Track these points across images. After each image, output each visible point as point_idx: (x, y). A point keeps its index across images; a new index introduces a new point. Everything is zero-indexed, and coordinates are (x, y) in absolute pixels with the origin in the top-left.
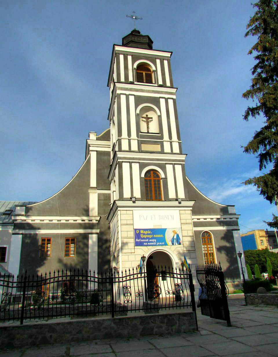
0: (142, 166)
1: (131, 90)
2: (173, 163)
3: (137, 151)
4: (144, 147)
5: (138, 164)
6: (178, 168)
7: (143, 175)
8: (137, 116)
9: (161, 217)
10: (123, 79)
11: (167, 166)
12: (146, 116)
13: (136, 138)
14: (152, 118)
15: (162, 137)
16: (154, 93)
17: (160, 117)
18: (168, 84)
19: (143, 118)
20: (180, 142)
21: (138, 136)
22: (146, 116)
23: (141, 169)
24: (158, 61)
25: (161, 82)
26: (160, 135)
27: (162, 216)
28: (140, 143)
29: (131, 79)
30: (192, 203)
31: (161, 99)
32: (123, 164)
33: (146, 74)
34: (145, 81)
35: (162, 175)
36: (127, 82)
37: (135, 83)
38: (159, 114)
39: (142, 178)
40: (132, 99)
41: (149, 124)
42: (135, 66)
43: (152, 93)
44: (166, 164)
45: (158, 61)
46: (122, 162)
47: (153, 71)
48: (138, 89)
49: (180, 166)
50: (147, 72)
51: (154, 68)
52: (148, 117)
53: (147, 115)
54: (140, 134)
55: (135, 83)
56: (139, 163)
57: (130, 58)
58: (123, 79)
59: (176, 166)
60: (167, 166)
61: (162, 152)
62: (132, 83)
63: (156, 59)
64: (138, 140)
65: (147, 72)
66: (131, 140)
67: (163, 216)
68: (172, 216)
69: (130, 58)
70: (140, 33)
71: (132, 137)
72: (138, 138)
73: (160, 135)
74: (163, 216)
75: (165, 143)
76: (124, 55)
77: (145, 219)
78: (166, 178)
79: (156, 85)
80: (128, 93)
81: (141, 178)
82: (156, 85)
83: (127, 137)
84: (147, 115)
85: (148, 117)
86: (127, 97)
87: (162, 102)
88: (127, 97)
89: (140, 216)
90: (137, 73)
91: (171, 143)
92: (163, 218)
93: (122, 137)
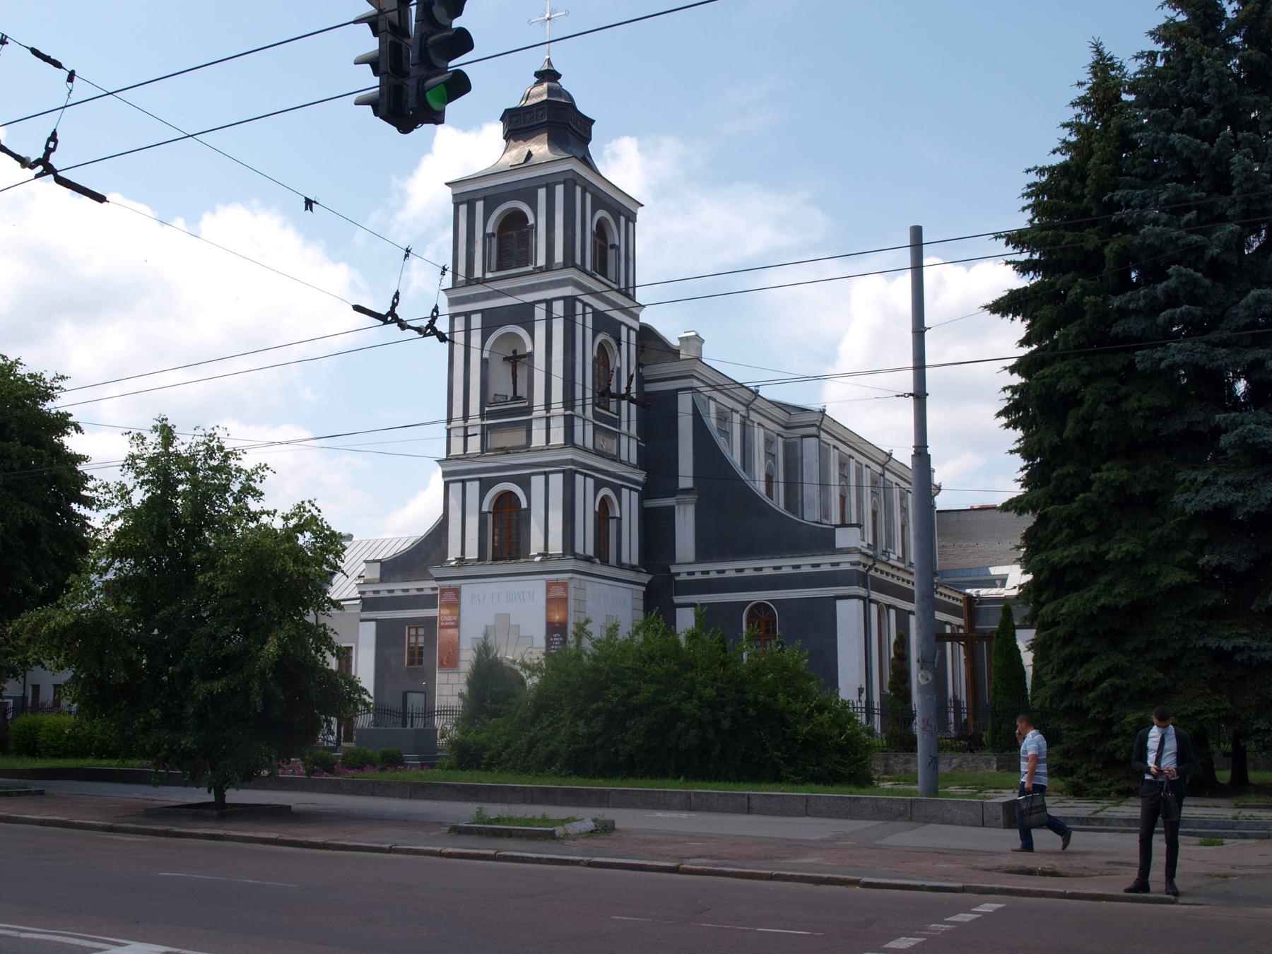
0: (599, 485)
2: (631, 485)
6: (635, 495)
10: (578, 261)
15: (617, 423)
21: (595, 413)
24: (623, 219)
30: (646, 578)
38: (618, 365)
44: (623, 486)
45: (623, 219)
46: (576, 472)
47: (613, 246)
51: (617, 243)
54: (597, 409)
58: (578, 261)
61: (615, 459)
73: (618, 417)
78: (620, 519)
79: (615, 286)
81: (595, 512)
82: (615, 286)
83: (581, 413)
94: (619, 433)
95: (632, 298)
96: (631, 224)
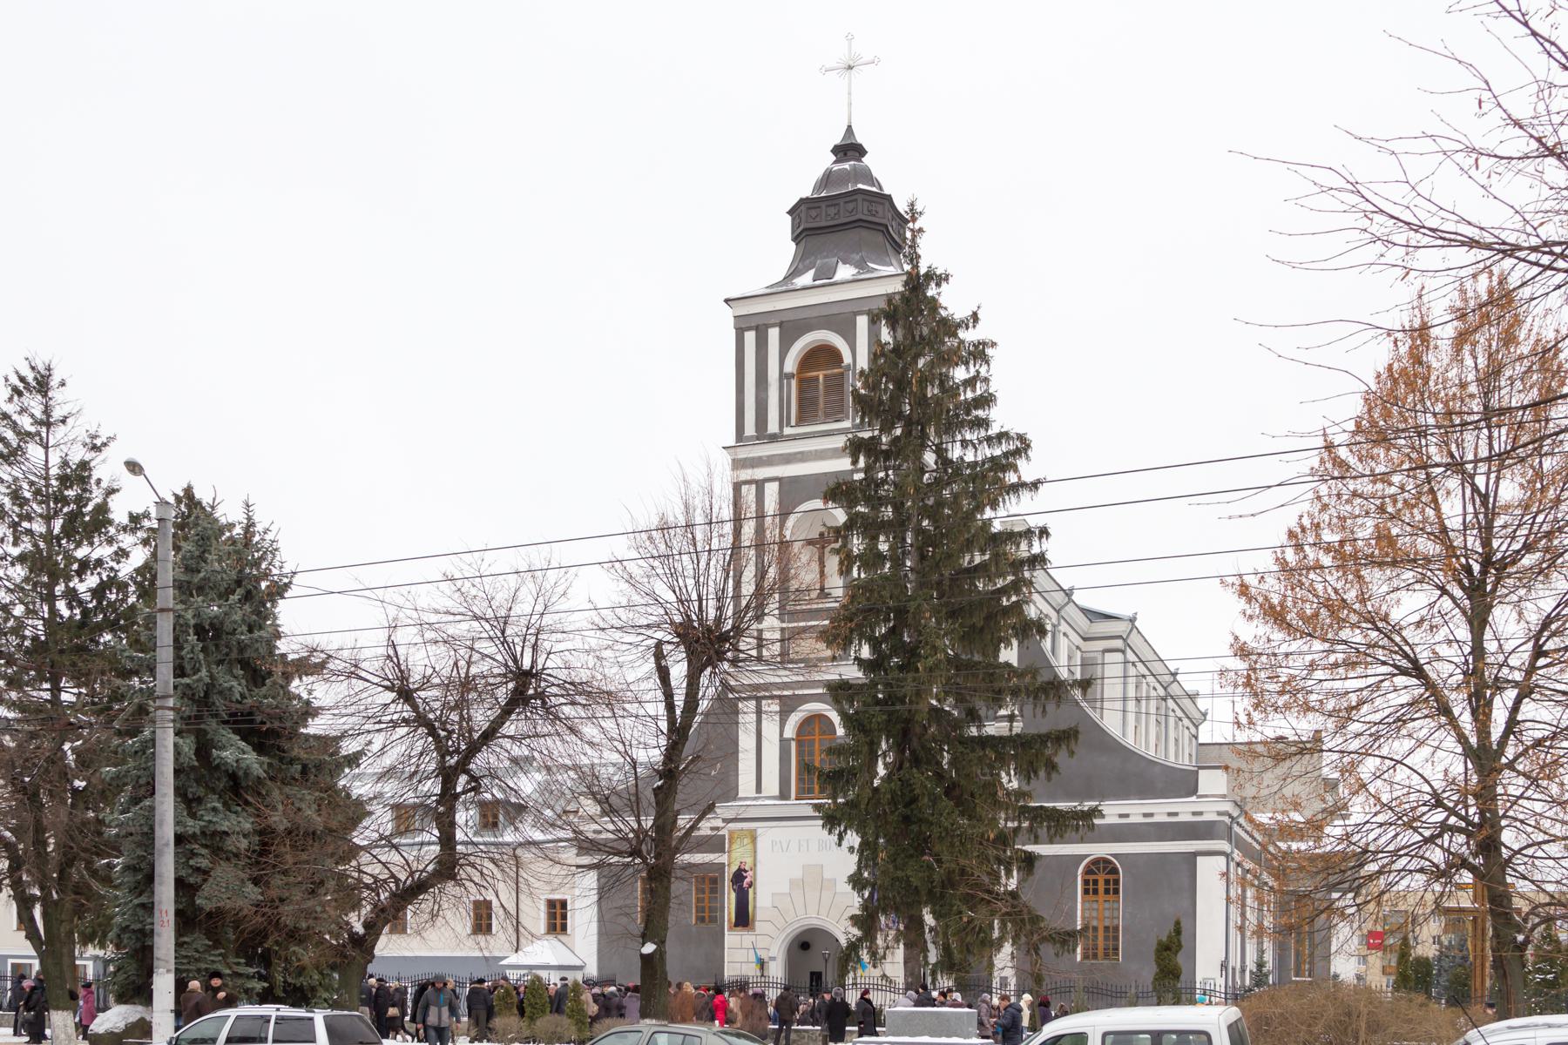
7: (790, 732)
23: (784, 715)
33: (825, 376)
37: (787, 431)
39: (789, 740)
42: (791, 365)
43: (831, 458)
48: (790, 454)
50: (829, 372)
55: (787, 431)
56: (780, 697)
57: (774, 334)
65: (829, 372)
69: (774, 334)
76: (757, 328)
77: (785, 847)
86: (760, 485)
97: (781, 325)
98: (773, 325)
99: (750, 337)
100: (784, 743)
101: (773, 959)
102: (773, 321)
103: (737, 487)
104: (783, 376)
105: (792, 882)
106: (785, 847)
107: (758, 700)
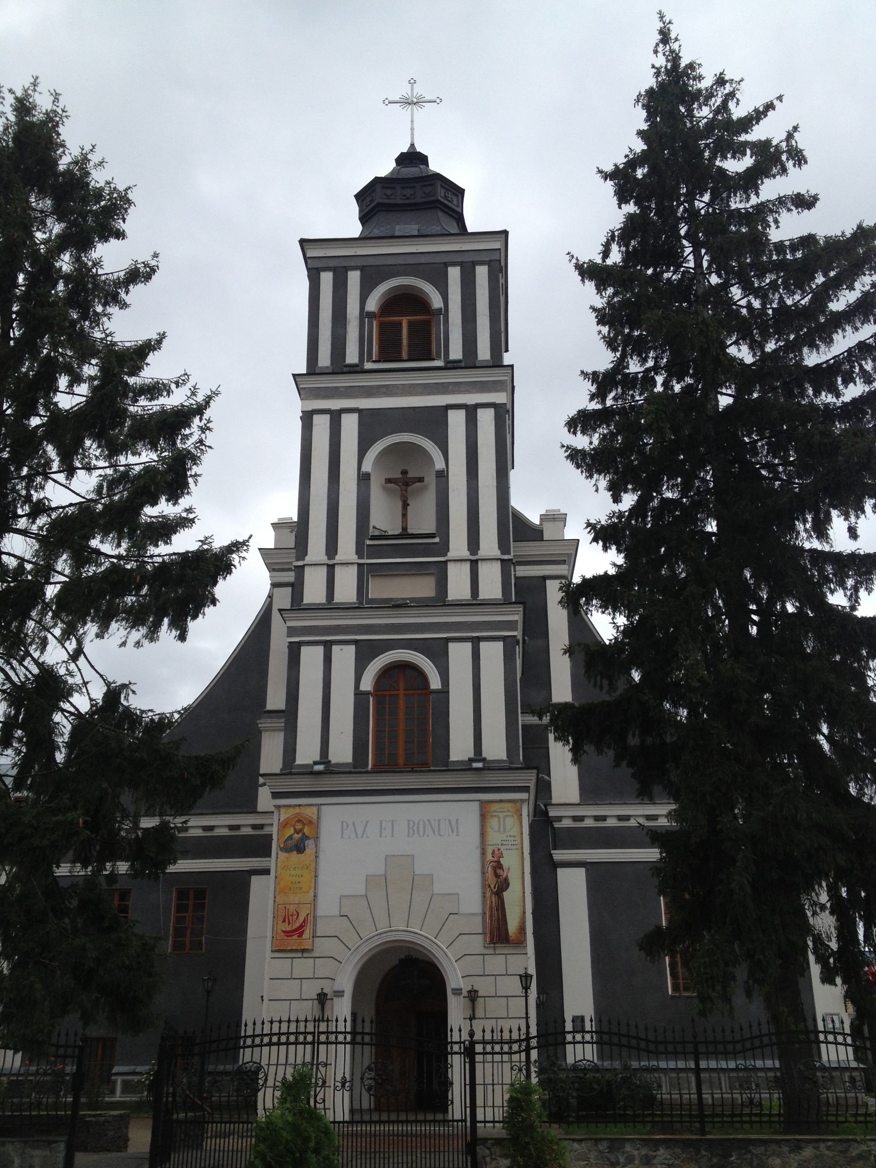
1: (348, 392)
3: (354, 603)
4: (378, 589)
5: (352, 648)
7: (367, 685)
8: (364, 479)
9: (415, 828)
11: (451, 646)
12: (400, 476)
13: (354, 558)
14: (421, 480)
15: (444, 547)
16: (429, 394)
17: (442, 476)
18: (484, 352)
19: (391, 483)
20: (506, 557)
21: (359, 552)
22: (400, 476)
24: (454, 274)
25: (456, 352)
26: (437, 540)
27: (416, 824)
28: (364, 573)
29: (352, 356)
31: (451, 413)
32: (304, 650)
33: (411, 324)
34: (405, 355)
35: (435, 683)
36: (340, 367)
38: (439, 465)
39: (367, 693)
40: (350, 425)
41: (409, 501)
42: (372, 305)
45: (454, 274)
46: (300, 644)
49: (500, 645)
52: (409, 475)
53: (405, 472)
54: (368, 542)
55: (368, 366)
56: (356, 642)
57: (354, 278)
58: (324, 360)
59: (483, 645)
60: (451, 646)
62: (356, 370)
63: (446, 265)
64: (359, 565)
66: (336, 566)
67: (421, 823)
68: (454, 823)
69: (354, 278)
70: (427, 157)
71: (339, 558)
72: (360, 557)
73: (437, 540)
74: (421, 823)
75: (452, 569)
77: (360, 834)
78: (444, 693)
79: (439, 363)
80: (335, 404)
82: (439, 363)
83: (323, 558)
84: (405, 472)
85: (409, 475)
86: (336, 417)
87: (457, 421)
88: (336, 417)
89: (345, 824)
90: (381, 326)
91: (474, 564)
92: (421, 832)
93: (308, 559)
94: (446, 562)
95: (496, 362)
96: (482, 273)
97: (362, 269)
98: (354, 268)
99: (327, 279)
100: (360, 697)
101: (340, 994)
102: (353, 264)
103: (307, 418)
104: (364, 315)
105: (369, 879)
106: (360, 834)
107: (328, 646)
